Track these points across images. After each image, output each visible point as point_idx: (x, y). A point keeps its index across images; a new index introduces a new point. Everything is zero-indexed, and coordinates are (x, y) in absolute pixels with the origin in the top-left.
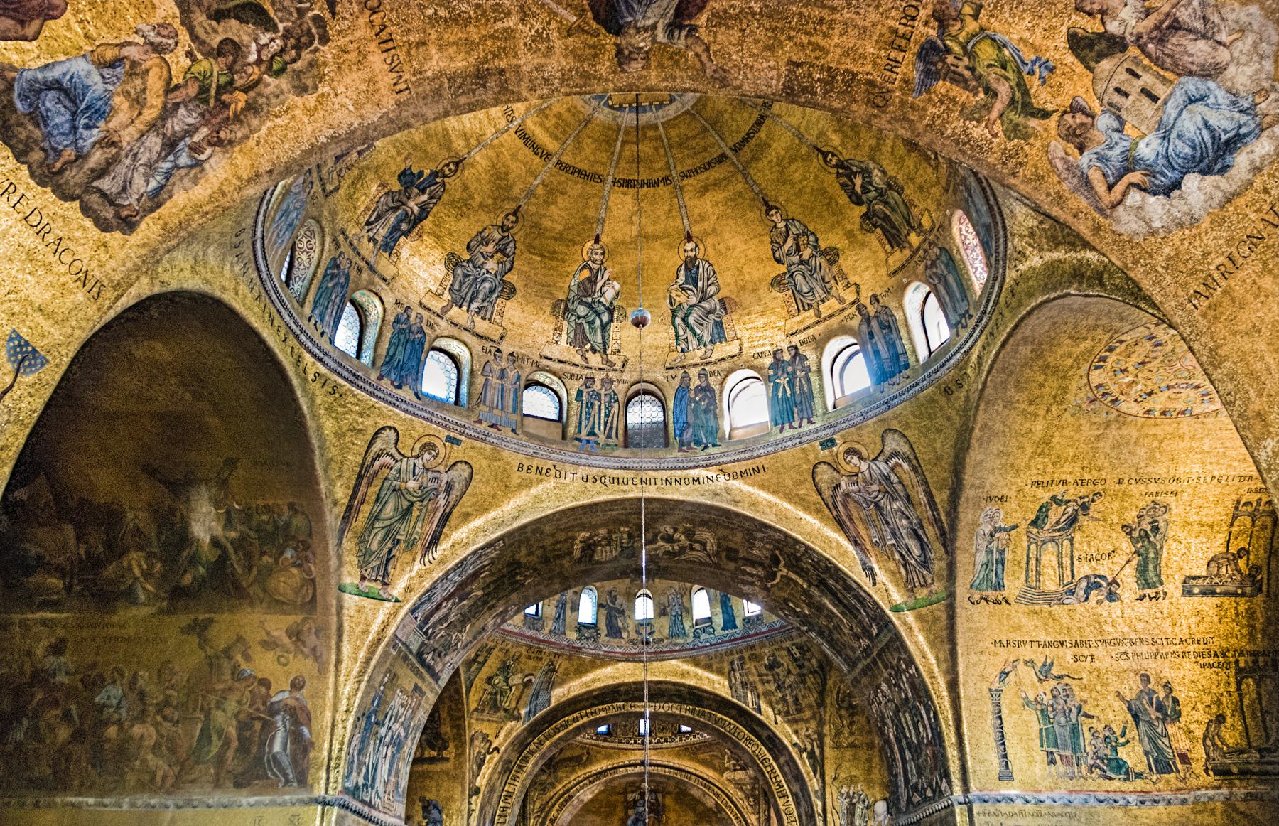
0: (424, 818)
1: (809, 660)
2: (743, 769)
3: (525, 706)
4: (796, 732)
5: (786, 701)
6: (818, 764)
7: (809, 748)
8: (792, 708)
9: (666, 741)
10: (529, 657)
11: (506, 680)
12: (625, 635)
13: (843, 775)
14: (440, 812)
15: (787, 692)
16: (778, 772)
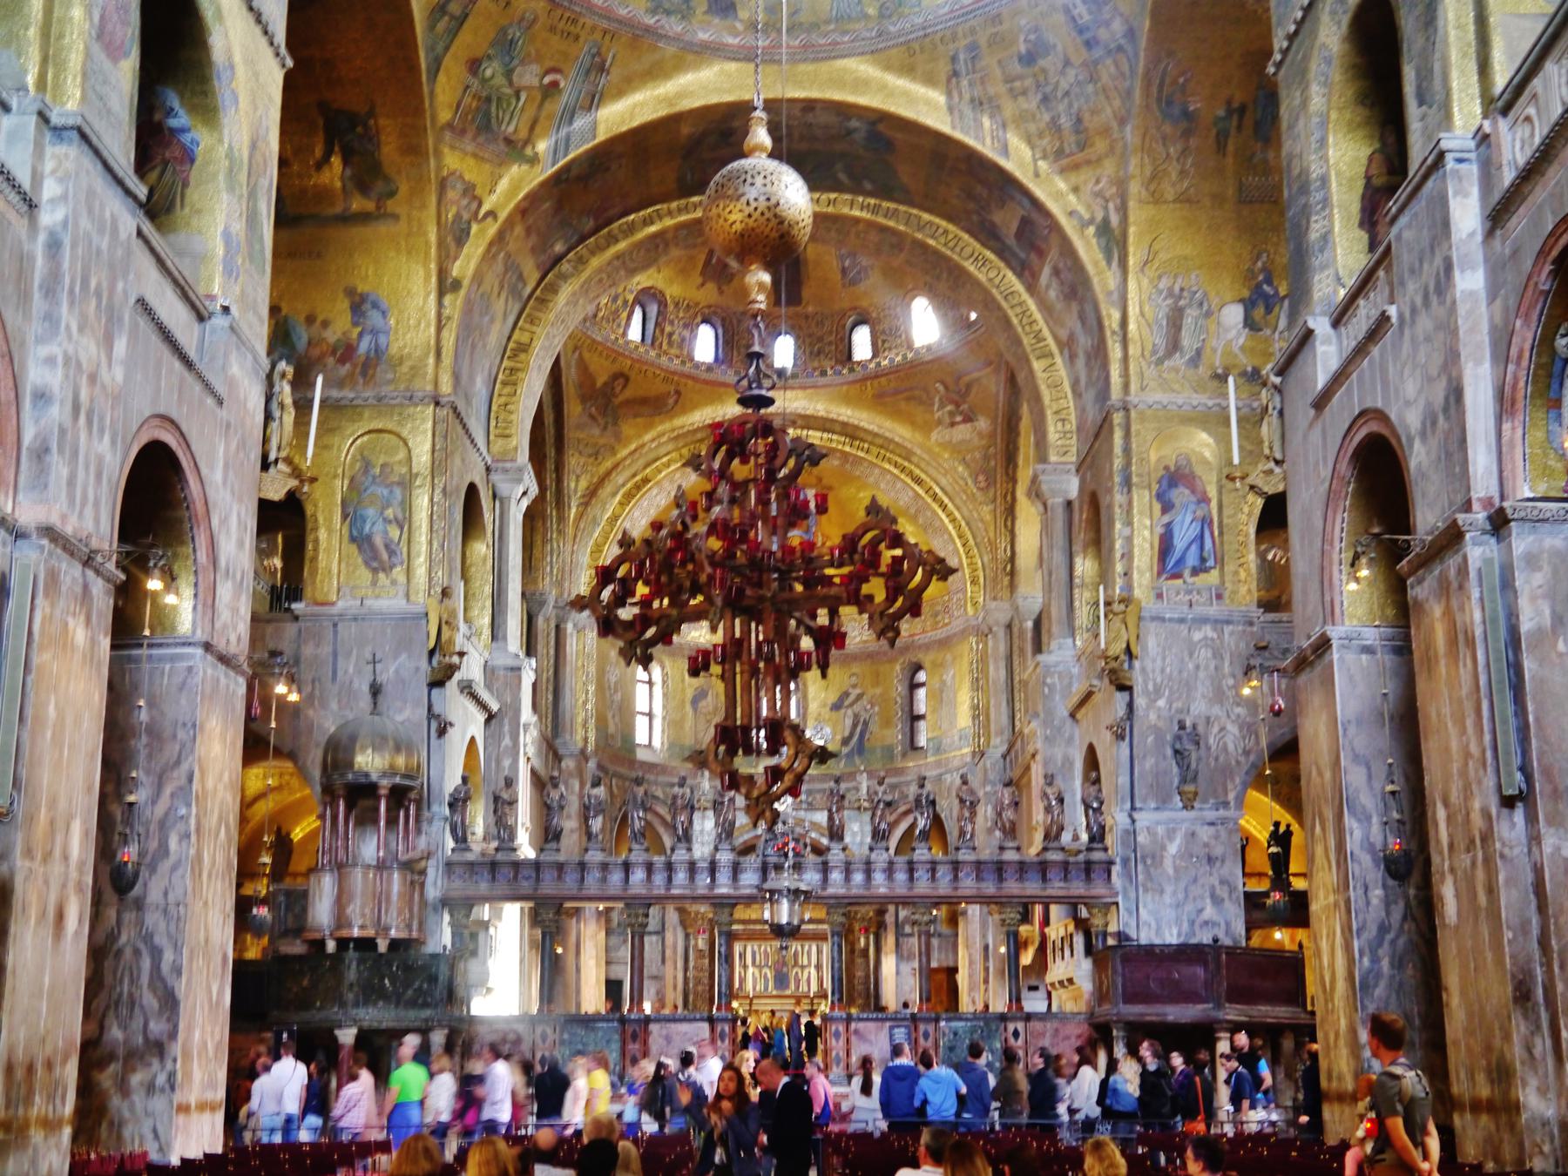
0: (355, 324)
1: (1107, 24)
2: (968, 419)
3: (544, 135)
4: (1076, 190)
5: (1059, 129)
6: (1113, 241)
7: (1099, 216)
8: (1070, 140)
9: (824, 373)
10: (552, 29)
11: (509, 74)
12: (743, 14)
13: (1163, 256)
14: (384, 314)
15: (1062, 107)
16: (1038, 316)
